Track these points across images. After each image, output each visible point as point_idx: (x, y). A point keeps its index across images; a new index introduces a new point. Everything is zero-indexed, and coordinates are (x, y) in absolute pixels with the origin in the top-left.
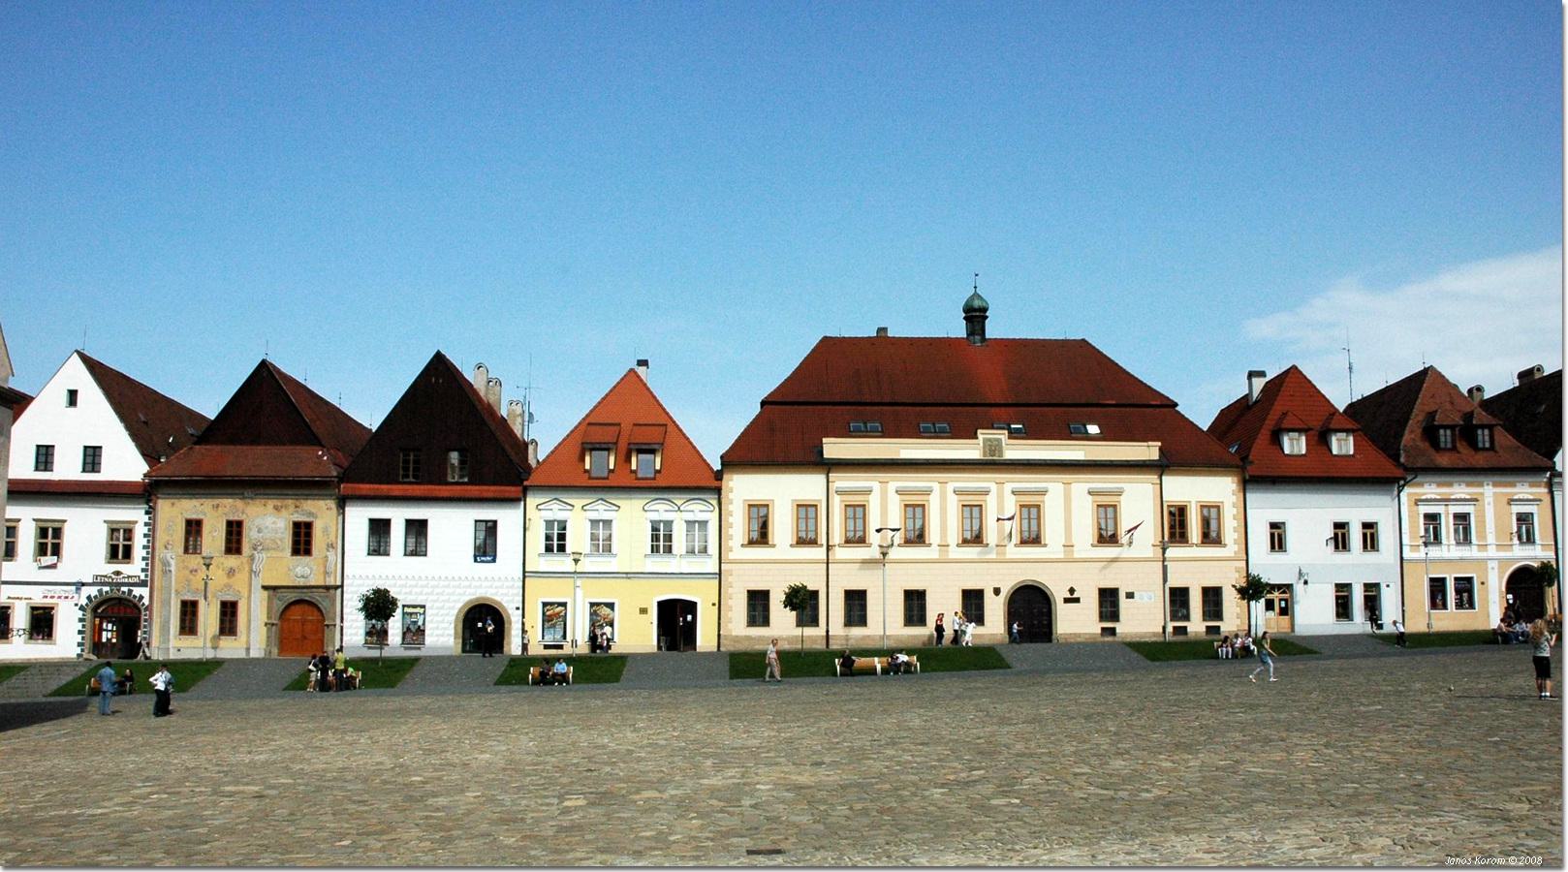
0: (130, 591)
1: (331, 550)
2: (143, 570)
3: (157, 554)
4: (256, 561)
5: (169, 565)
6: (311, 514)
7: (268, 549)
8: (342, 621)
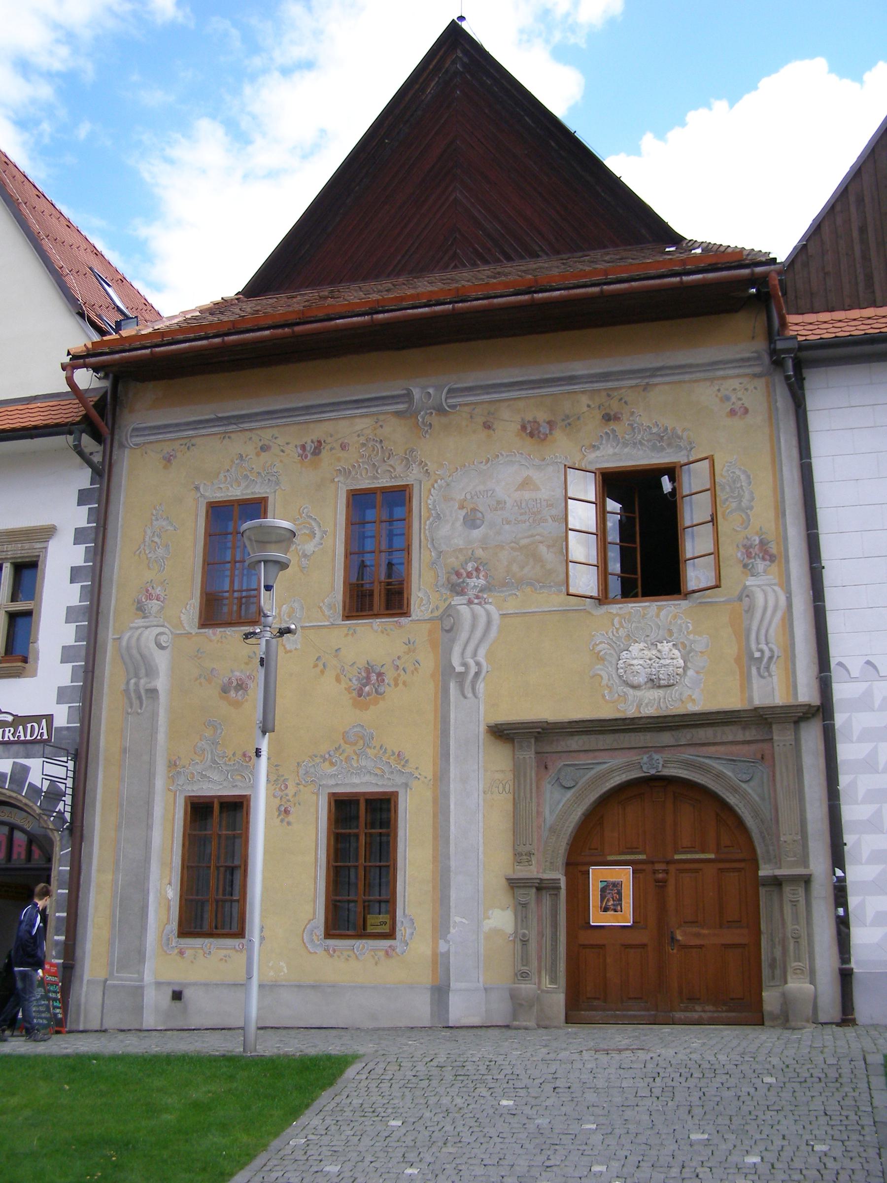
0: (21, 773)
1: (760, 566)
2: (62, 695)
3: (111, 636)
4: (464, 636)
5: (151, 672)
6: (665, 438)
7: (504, 584)
8: (838, 858)
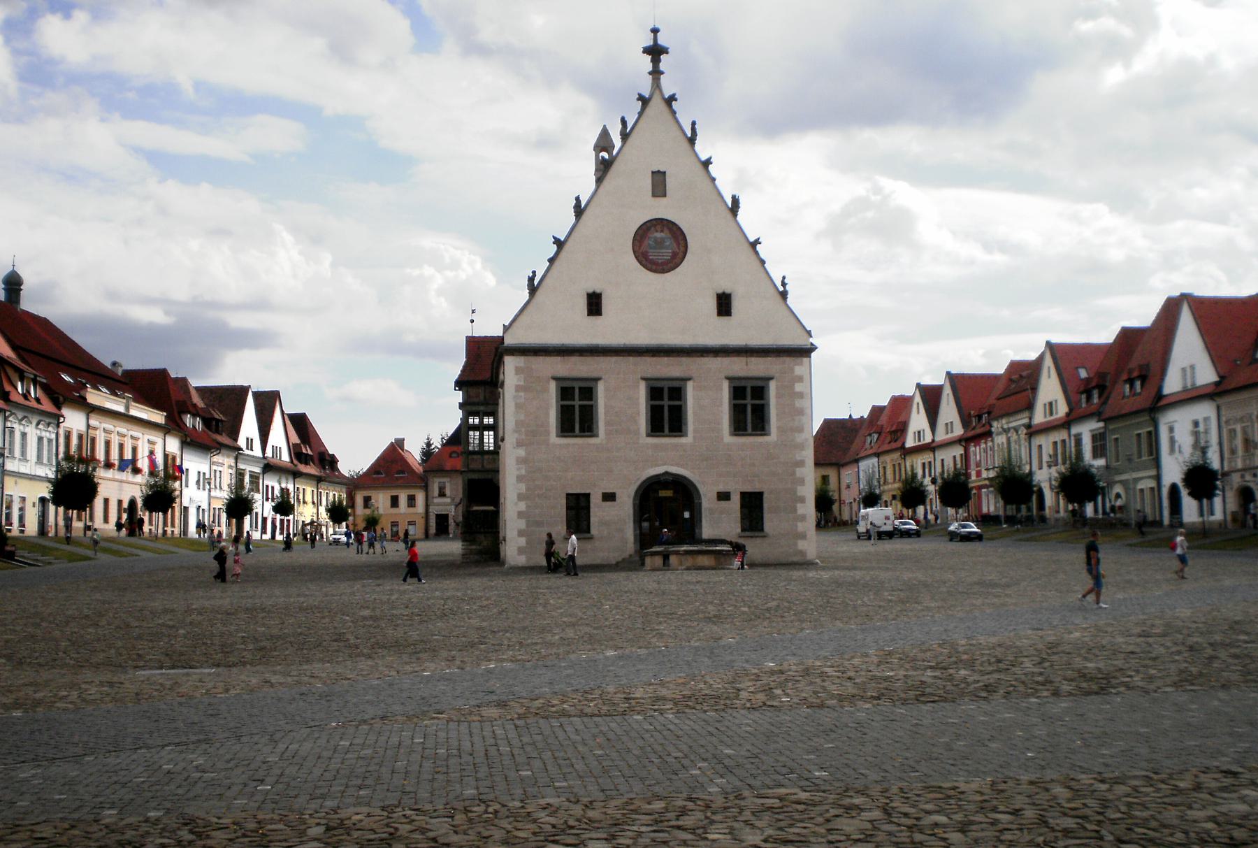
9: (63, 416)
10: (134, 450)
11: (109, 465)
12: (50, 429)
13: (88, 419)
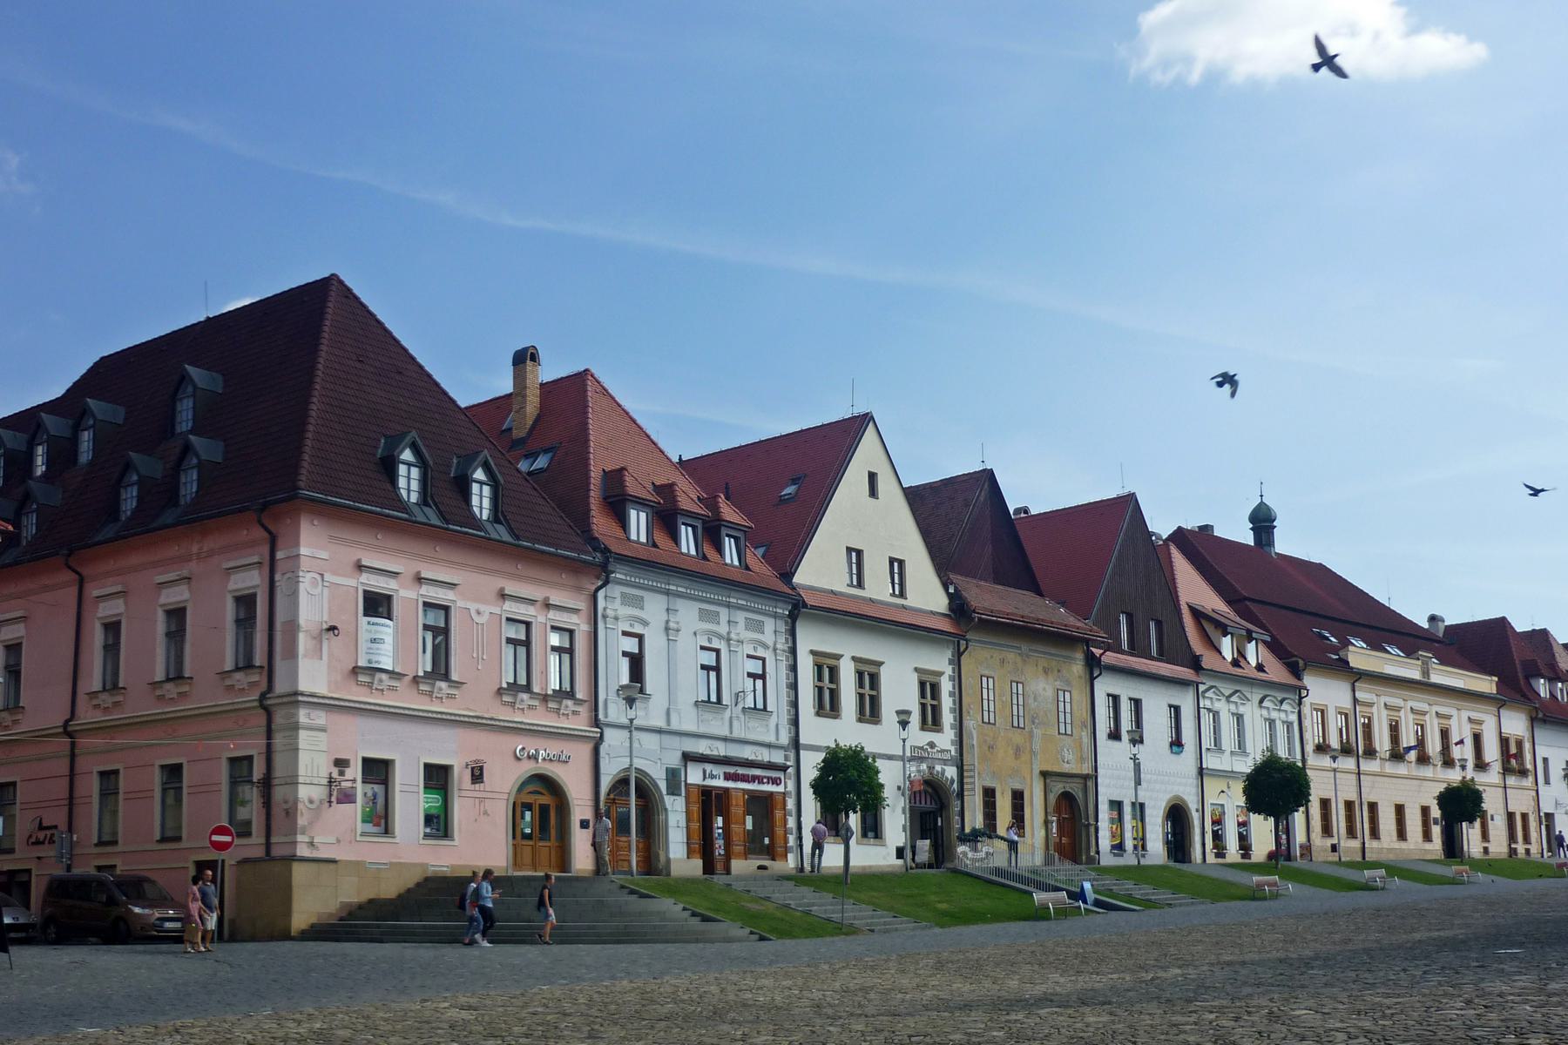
0: (943, 771)
8: (1097, 821)
9: (1305, 689)
10: (1445, 734)
11: (1397, 756)
12: (1285, 706)
13: (1354, 691)
